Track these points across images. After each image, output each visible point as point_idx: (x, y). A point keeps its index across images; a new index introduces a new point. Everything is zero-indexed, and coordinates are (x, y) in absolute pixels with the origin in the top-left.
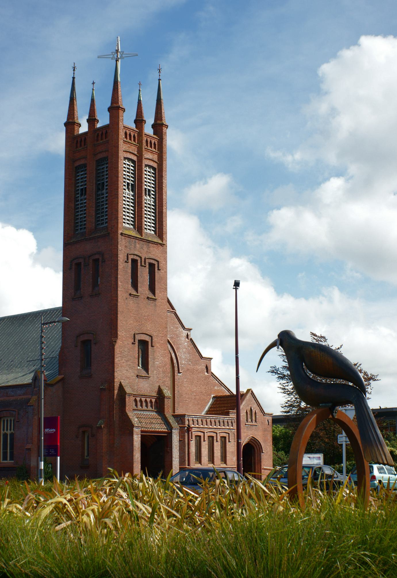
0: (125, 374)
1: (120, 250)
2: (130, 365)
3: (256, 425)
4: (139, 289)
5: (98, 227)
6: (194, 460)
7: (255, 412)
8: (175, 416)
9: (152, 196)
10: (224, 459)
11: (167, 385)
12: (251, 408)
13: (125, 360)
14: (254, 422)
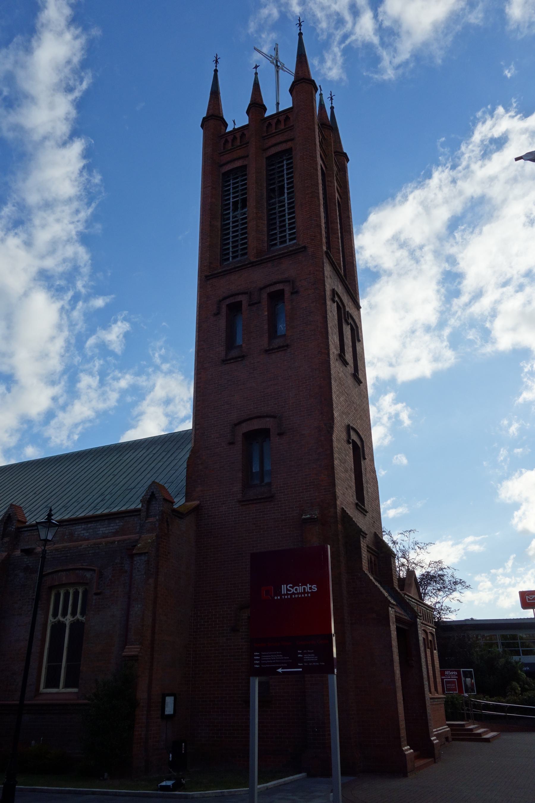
5: (272, 249)
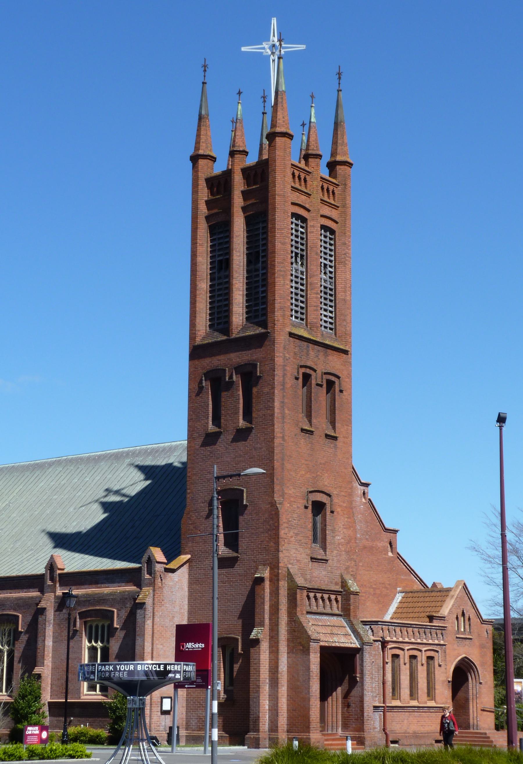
0: (294, 555)
2: (300, 541)
3: (471, 639)
4: (314, 421)
6: (391, 694)
7: (469, 617)
8: (365, 623)
9: (329, 274)
10: (430, 692)
11: (352, 573)
12: (463, 611)
13: (294, 533)
14: (467, 634)
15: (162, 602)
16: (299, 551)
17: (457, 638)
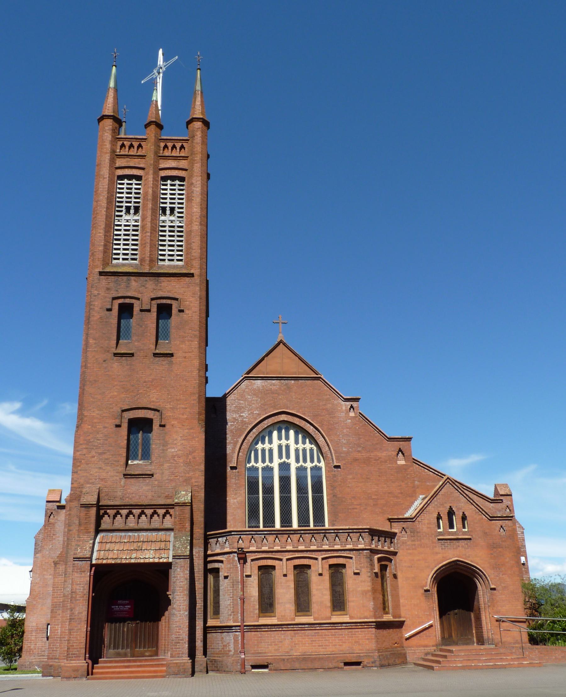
1: (95, 296)
2: (107, 459)
3: (470, 539)
13: (96, 453)
15: (52, 537)
16: (104, 470)
17: (439, 539)
